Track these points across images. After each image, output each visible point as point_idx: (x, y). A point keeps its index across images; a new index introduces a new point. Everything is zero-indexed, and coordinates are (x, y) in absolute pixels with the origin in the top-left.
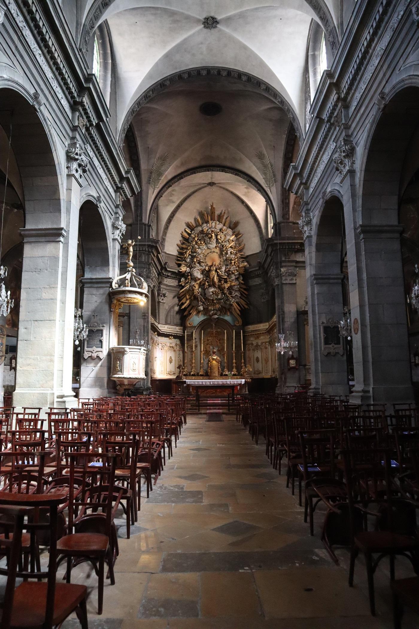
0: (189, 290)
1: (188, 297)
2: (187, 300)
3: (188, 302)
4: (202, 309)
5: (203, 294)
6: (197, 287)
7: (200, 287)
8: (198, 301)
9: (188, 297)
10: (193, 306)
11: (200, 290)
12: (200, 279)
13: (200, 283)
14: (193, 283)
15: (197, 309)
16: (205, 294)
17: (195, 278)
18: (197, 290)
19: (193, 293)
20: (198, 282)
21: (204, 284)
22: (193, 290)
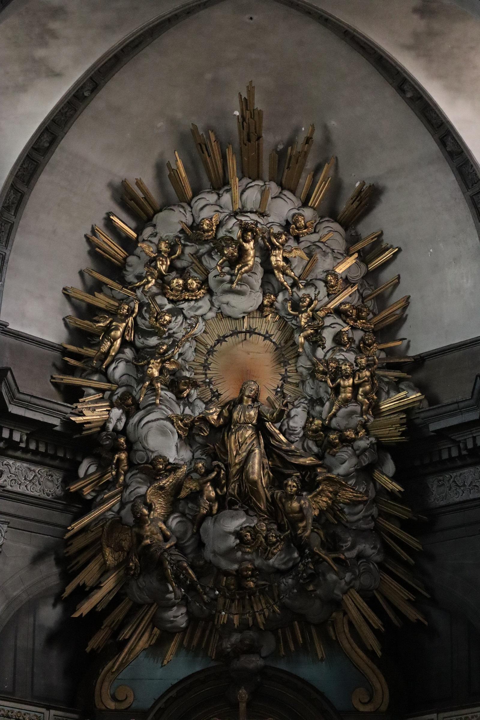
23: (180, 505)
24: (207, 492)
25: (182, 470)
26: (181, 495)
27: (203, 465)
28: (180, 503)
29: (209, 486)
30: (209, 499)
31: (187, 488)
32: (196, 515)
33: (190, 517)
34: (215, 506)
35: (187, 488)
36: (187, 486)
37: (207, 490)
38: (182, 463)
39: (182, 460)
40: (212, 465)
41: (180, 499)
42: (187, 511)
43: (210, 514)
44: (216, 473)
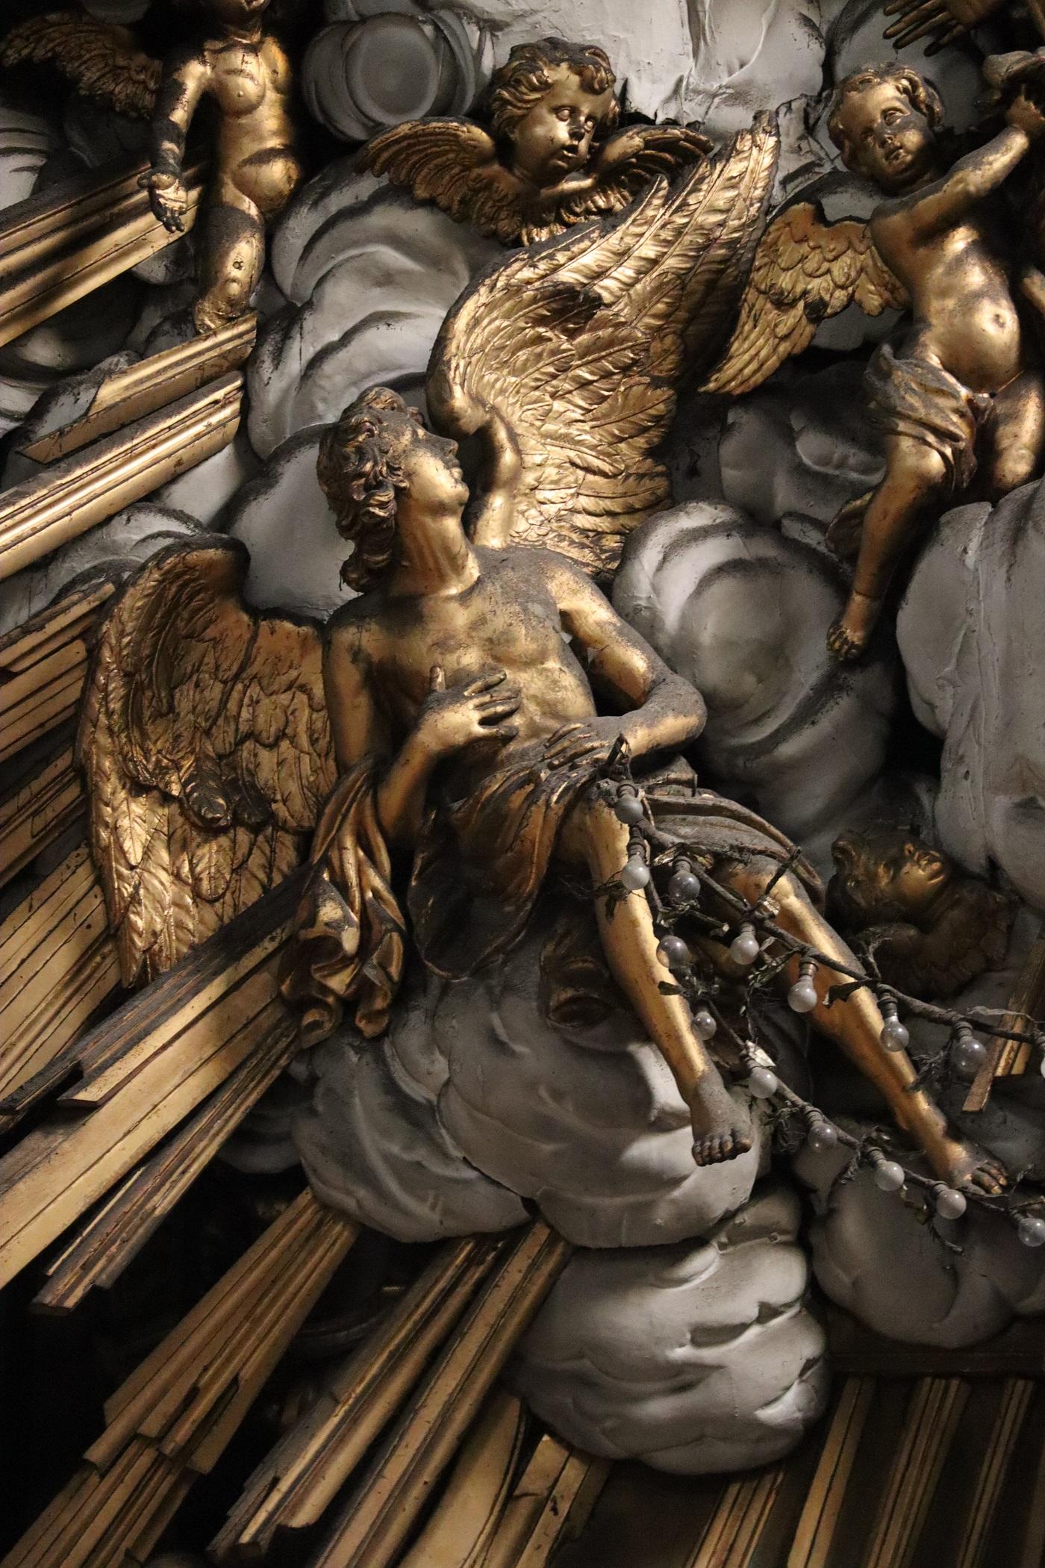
0: (221, 575)
1: (157, 871)
2: (116, 985)
3: (160, 1081)
4: (772, 1376)
5: (820, 749)
6: (560, 457)
7: (677, 454)
8: (606, 1011)
9: (157, 871)
10: (380, 1269)
11: (684, 567)
12: (679, 157)
13: (708, 301)
14: (388, 316)
15: (529, 1394)
16: (909, 752)
17: (499, 103)
18: (567, 577)
19: (399, 697)
20: (620, 257)
21: (839, 379)
22: (393, 566)
23: (729, 449)
24: (950, 303)
25: (734, 168)
26: (730, 369)
27: (911, 95)
28: (726, 429)
29: (959, 261)
30: (970, 364)
31: (782, 303)
32: (859, 514)
33: (813, 538)
34: (1015, 417)
35: (782, 303)
36: (785, 281)
37: (944, 293)
38: (737, 117)
39: (738, 96)
40: (986, 85)
41: (725, 401)
42: (785, 495)
43: (976, 477)
44: (1018, 142)
